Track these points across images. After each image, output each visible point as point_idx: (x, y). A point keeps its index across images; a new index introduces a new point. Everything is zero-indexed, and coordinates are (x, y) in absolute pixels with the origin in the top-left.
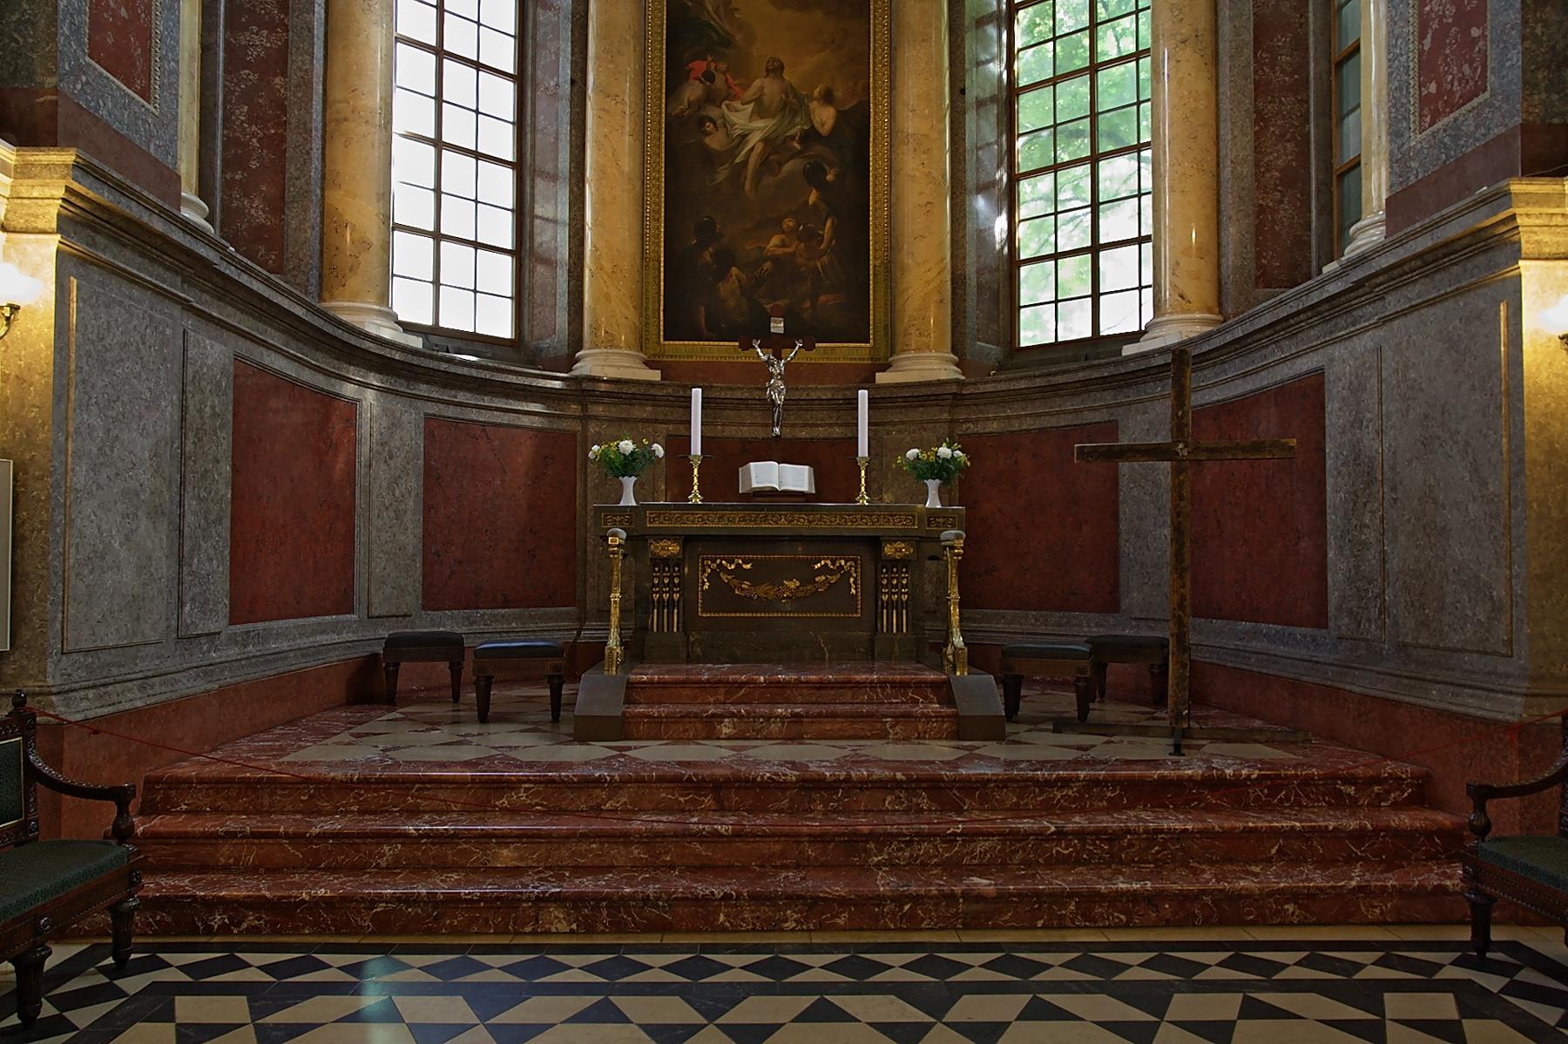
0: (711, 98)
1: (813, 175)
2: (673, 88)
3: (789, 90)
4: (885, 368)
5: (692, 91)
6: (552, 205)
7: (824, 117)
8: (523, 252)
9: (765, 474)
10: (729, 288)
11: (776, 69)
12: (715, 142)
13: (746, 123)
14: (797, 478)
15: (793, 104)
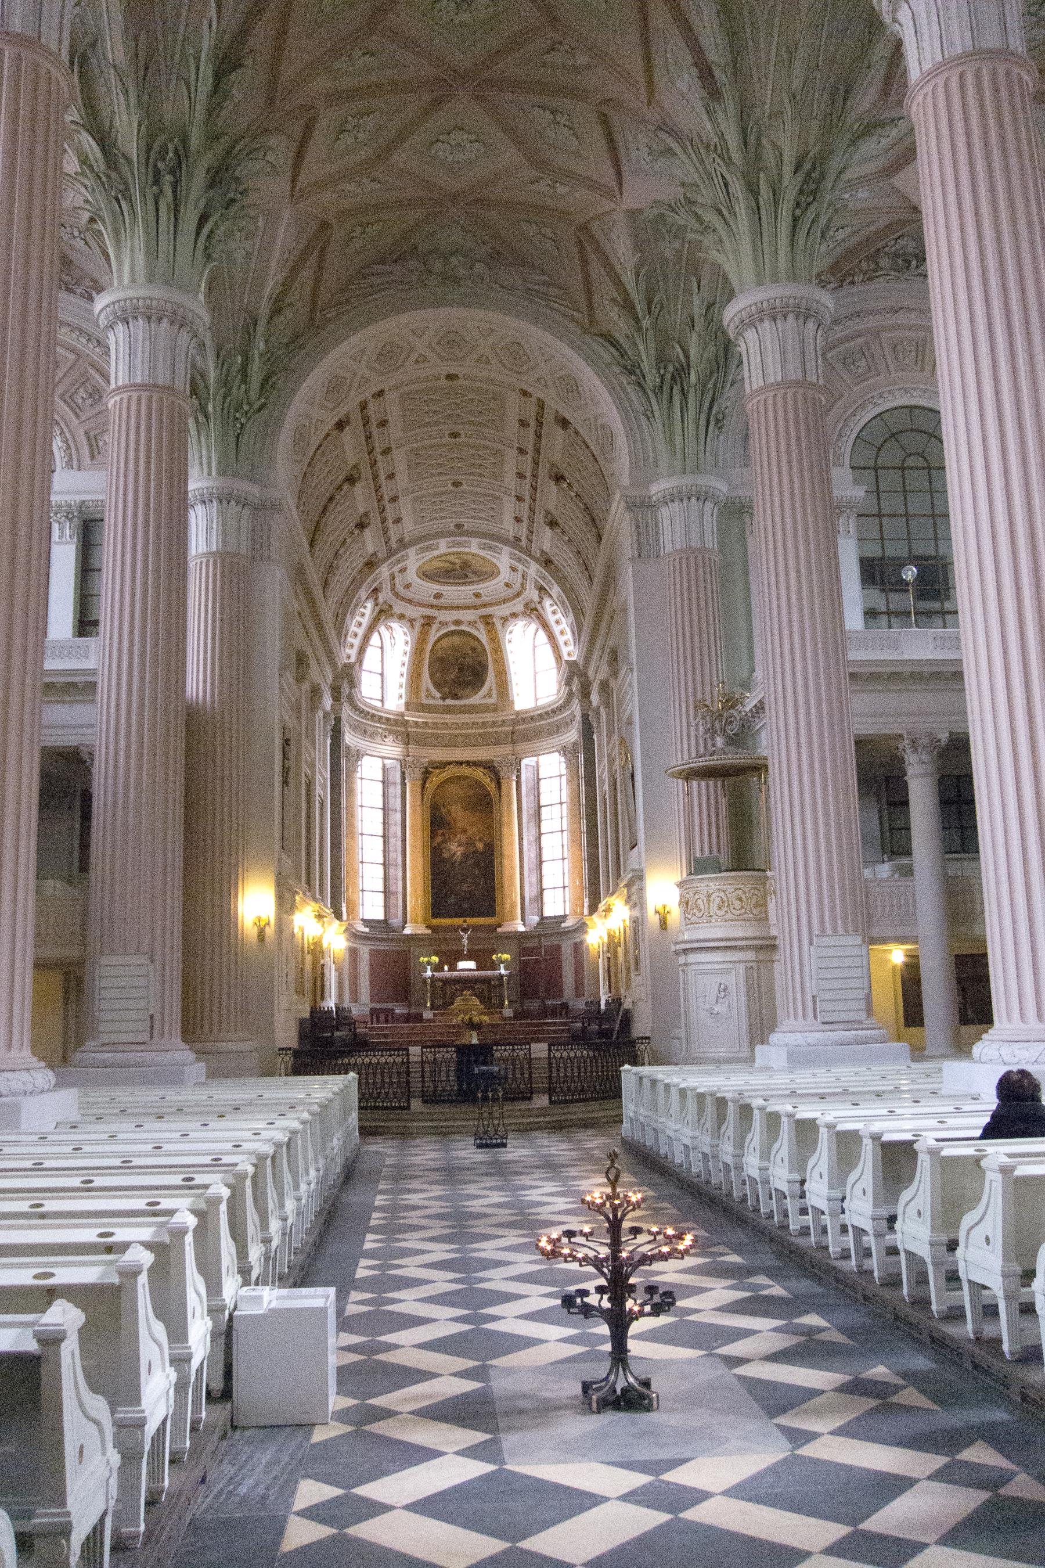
0: (444, 841)
1: (477, 864)
2: (432, 838)
3: (469, 838)
4: (500, 926)
5: (439, 839)
6: (396, 873)
7: (480, 846)
8: (387, 892)
9: (462, 965)
10: (452, 900)
11: (464, 831)
12: (446, 855)
13: (455, 849)
14: (471, 965)
15: (470, 843)
